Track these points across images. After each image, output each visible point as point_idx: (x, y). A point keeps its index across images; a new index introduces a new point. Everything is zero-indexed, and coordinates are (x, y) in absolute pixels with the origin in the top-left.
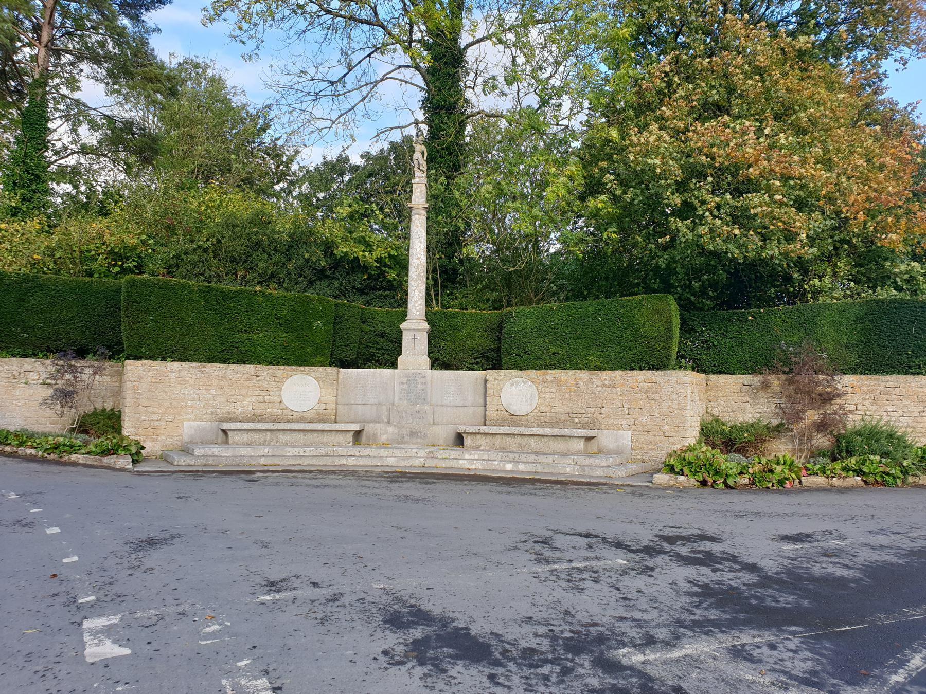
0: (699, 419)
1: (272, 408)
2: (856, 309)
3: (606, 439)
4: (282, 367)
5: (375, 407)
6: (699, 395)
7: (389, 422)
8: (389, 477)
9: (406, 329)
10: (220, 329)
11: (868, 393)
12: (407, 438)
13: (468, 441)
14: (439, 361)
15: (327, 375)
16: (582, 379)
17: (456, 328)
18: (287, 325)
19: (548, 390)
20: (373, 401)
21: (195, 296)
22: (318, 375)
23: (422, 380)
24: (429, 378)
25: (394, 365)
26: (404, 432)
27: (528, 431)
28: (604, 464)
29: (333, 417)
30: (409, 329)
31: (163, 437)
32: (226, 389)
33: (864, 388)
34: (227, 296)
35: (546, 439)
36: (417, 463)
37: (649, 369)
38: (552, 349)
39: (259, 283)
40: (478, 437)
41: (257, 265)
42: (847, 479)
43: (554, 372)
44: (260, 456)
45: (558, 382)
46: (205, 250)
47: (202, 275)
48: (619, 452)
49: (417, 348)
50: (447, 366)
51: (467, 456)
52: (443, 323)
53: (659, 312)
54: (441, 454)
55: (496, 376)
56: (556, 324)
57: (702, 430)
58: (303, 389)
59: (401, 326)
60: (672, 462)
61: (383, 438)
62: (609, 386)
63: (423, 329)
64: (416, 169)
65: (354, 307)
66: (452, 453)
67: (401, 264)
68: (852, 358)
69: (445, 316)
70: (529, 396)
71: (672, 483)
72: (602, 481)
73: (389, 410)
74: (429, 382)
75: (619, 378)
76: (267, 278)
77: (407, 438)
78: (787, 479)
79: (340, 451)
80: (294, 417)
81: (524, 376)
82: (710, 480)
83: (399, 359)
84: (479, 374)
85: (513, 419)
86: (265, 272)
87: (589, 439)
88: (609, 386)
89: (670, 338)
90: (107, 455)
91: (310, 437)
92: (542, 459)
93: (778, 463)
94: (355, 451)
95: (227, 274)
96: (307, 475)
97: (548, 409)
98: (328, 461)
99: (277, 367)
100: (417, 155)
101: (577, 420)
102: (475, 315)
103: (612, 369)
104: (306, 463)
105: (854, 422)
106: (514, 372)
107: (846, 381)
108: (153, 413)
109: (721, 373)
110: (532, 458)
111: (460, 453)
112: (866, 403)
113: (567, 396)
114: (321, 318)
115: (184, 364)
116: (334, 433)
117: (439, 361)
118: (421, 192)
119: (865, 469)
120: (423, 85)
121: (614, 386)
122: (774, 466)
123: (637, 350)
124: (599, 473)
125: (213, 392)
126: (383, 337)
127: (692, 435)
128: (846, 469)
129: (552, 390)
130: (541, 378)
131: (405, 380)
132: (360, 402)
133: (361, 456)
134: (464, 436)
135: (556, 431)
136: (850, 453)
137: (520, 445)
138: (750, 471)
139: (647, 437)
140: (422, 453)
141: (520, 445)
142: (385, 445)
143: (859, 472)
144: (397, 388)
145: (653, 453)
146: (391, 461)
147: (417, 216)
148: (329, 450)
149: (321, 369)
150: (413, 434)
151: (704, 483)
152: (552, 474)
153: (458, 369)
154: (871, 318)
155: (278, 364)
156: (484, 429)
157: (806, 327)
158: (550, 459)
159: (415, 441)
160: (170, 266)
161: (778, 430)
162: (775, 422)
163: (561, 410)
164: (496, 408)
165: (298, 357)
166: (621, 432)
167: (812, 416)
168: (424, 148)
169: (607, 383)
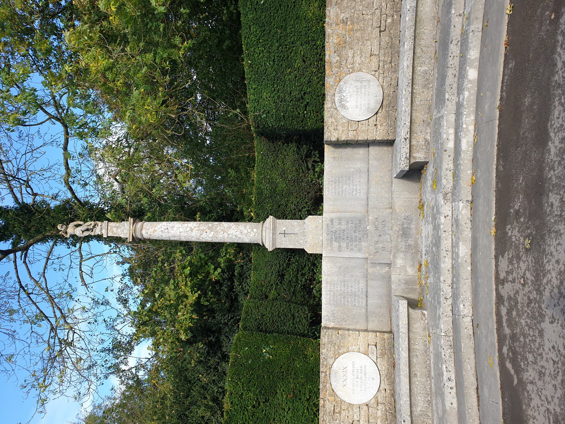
4: (321, 402)
5: (370, 282)
7: (389, 265)
12: (411, 242)
15: (330, 342)
16: (337, 16)
17: (274, 190)
19: (350, 60)
20: (362, 285)
22: (331, 354)
23: (336, 223)
24: (333, 215)
26: (402, 245)
29: (386, 335)
30: (274, 240)
35: (418, 50)
38: (298, 63)
40: (414, 142)
41: (203, 417)
43: (327, 53)
49: (296, 230)
51: (451, 145)
55: (331, 128)
59: (270, 249)
61: (411, 271)
63: (274, 224)
69: (260, 203)
70: (359, 84)
74: (338, 215)
77: (411, 242)
79: (445, 325)
80: (387, 387)
81: (332, 92)
83: (309, 251)
86: (211, 407)
91: (418, 369)
94: (446, 307)
97: (374, 59)
98: (467, 346)
99: (321, 409)
101: (389, 20)
110: (454, 49)
113: (358, 34)
114: (259, 348)
118: (118, 228)
126: (283, 275)
129: (350, 53)
130: (335, 70)
131: (335, 244)
134: (413, 161)
137: (425, 86)
141: (425, 86)
144: (346, 254)
147: (144, 232)
148: (445, 343)
149: (323, 351)
150: (405, 233)
153: (321, 190)
155: (317, 406)
158: (457, 22)
159: (414, 231)
163: (376, 43)
164: (372, 128)
168: (72, 225)
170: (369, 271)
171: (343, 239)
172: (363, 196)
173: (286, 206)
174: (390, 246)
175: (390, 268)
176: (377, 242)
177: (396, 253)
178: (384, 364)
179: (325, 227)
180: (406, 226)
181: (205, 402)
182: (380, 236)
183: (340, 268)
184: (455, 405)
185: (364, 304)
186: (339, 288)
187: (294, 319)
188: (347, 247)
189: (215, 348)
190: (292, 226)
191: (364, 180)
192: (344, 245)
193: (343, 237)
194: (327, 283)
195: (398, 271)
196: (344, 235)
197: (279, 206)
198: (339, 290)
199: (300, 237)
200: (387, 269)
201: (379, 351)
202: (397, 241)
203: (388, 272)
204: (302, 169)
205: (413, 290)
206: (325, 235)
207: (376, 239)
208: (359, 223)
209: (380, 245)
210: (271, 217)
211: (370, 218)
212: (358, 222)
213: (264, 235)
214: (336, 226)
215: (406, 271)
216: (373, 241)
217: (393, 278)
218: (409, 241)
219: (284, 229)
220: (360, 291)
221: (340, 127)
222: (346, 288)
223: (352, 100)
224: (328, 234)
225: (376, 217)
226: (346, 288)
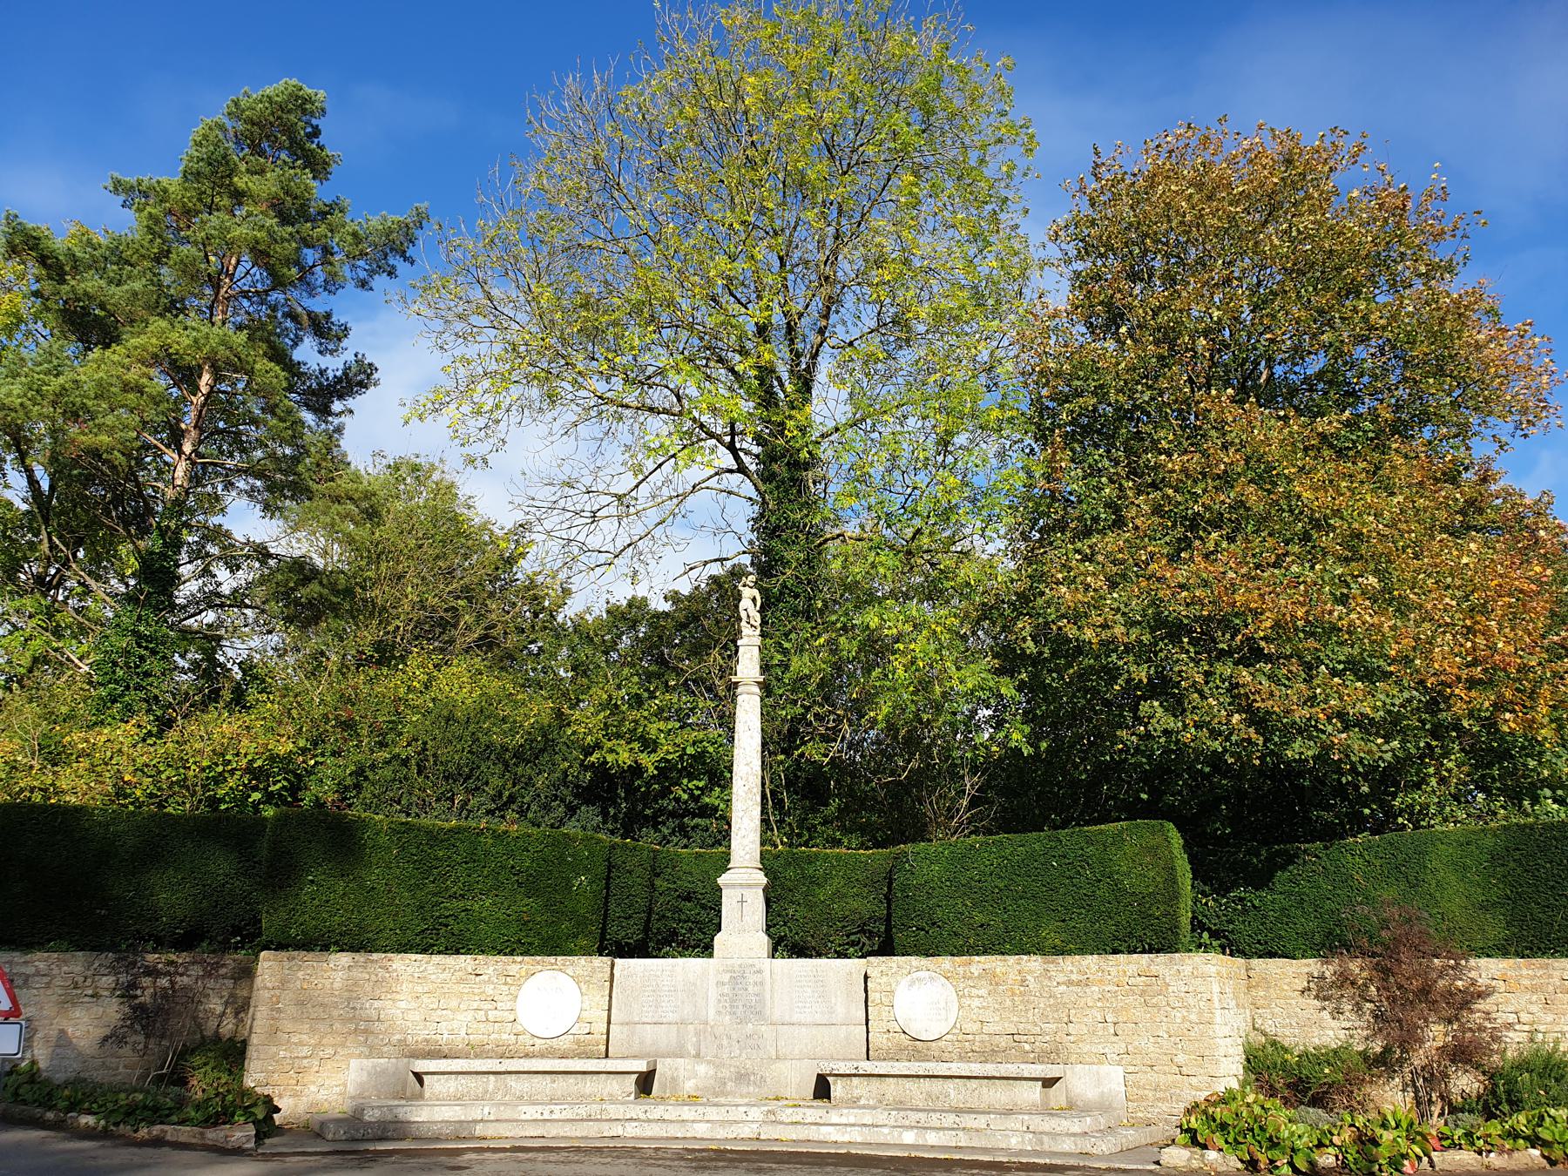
0: (1240, 1041)
1: (499, 1033)
2: (1489, 842)
3: (1081, 1081)
4: (519, 959)
6: (1236, 998)
7: (698, 1055)
8: (695, 1160)
9: (727, 886)
10: (419, 894)
11: (1534, 990)
13: (837, 1088)
14: (790, 940)
16: (1030, 972)
17: (814, 882)
18: (531, 886)
19: (974, 992)
20: (672, 1017)
21: (383, 839)
22: (579, 971)
23: (757, 978)
24: (767, 974)
25: (707, 950)
26: (725, 1073)
27: (942, 1069)
28: (1076, 1129)
30: (733, 886)
31: (313, 1088)
32: (425, 999)
33: (1526, 982)
34: (433, 837)
35: (974, 1083)
36: (746, 1131)
37: (1144, 952)
38: (979, 918)
39: (490, 812)
40: (855, 1080)
41: (487, 783)
42: (1516, 1155)
44: (475, 1122)
45: (991, 977)
46: (406, 762)
47: (399, 803)
48: (1104, 1107)
50: (799, 951)
51: (835, 1118)
52: (790, 873)
53: (1153, 851)
54: (788, 1115)
56: (982, 873)
57: (1248, 1060)
58: (552, 995)
59: (720, 881)
60: (1194, 1124)
61: (689, 1086)
62: (1079, 984)
63: (756, 885)
64: (743, 623)
65: (642, 849)
66: (809, 1112)
67: (719, 775)
68: (1496, 929)
69: (794, 861)
70: (943, 1004)
71: (1195, 1164)
72: (1072, 1162)
73: (697, 1034)
75: (1094, 968)
76: (501, 805)
78: (1405, 1156)
79: (614, 1111)
80: (537, 1048)
81: (931, 967)
82: (1263, 1159)
83: (718, 939)
84: (855, 966)
85: (917, 1047)
86: (500, 795)
87: (1049, 1083)
88: (1079, 984)
89: (1175, 896)
90: (215, 1124)
91: (562, 1083)
92: (968, 1121)
93: (1384, 1126)
94: (637, 1110)
95: (438, 800)
96: (553, 1157)
97: (975, 1027)
98: (591, 1130)
100: (745, 603)
101: (1027, 1047)
102: (849, 858)
103: (1082, 951)
104: (553, 1133)
105: (1515, 1043)
106: (914, 960)
107: (1486, 970)
108: (301, 1044)
109: (1272, 955)
110: (950, 1119)
111: (822, 1112)
112: (1534, 1008)
113: (1008, 1003)
114: (587, 871)
115: (357, 956)
116: (603, 1076)
117: (790, 940)
119: (1545, 1135)
120: (754, 494)
121: (1087, 983)
122: (1379, 1131)
123: (1122, 918)
124: (1067, 1145)
125: (403, 1005)
126: (688, 899)
127: (1229, 1073)
128: (1513, 1135)
129: (980, 992)
130: (961, 970)
133: (649, 1121)
134: (830, 1079)
135: (990, 1069)
136: (1516, 1105)
137: (929, 1095)
138: (1336, 1140)
139: (1152, 1077)
140: (756, 1113)
141: (929, 1095)
142: (692, 1100)
143: (1534, 1141)
144: (713, 993)
145: (1165, 1107)
146: (701, 1130)
148: (594, 1109)
149: (582, 961)
150: (742, 1077)
151: (1252, 1164)
152: (985, 1150)
153: (819, 955)
154: (1517, 855)
155: (511, 953)
156: (868, 1067)
157: (1407, 871)
158: (981, 1122)
159: (744, 1090)
160: (346, 788)
161: (1383, 1063)
162: (1377, 1047)
164: (884, 1026)
165: (547, 941)
166: (1105, 1068)
167: (1437, 1034)
168: (756, 592)
169: (1074, 977)
172: (794, 1020)
178: (565, 1044)
181: (509, 785)
184: (523, 1117)
189: (587, 795)
191: (819, 1018)
200: (693, 1053)
201: (582, 1038)
205: (663, 1086)
207: (734, 1036)
208: (756, 1011)
214: (752, 978)
221: (885, 979)
223: (924, 994)
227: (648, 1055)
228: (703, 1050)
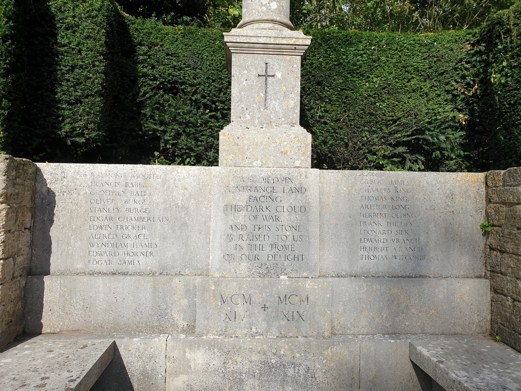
5: (147, 283)
7: (191, 329)
20: (144, 263)
24: (313, 194)
30: (250, 48)
49: (274, 104)
59: (227, 38)
73: (190, 292)
83: (225, 135)
131: (242, 198)
132: (103, 267)
144: (218, 225)
170: (177, 279)
171: (255, 217)
173: (321, 99)
174: (239, 333)
175: (184, 331)
176: (248, 300)
177: (220, 349)
179: (284, 172)
180: (291, 372)
182: (265, 308)
183: (185, 209)
185: (94, 267)
186: (132, 205)
187: (68, 103)
188: (235, 227)
190: (285, 96)
192: (241, 218)
193: (260, 218)
194: (145, 178)
195: (176, 354)
196: (265, 218)
197: (319, 83)
198: (128, 206)
199: (258, 115)
200: (182, 323)
202: (251, 350)
203: (175, 326)
204: (397, 132)
206: (265, 172)
207: (257, 298)
209: (241, 309)
210: (309, 42)
211: (309, 284)
212: (297, 253)
213: (263, 25)
214: (287, 201)
215: (176, 374)
216: (251, 292)
217: (159, 341)
218: (251, 382)
219: (279, 74)
220: (127, 258)
222: (134, 223)
224: (266, 180)
225: (311, 298)
226: (134, 223)
227: (100, 331)
228: (201, 323)
